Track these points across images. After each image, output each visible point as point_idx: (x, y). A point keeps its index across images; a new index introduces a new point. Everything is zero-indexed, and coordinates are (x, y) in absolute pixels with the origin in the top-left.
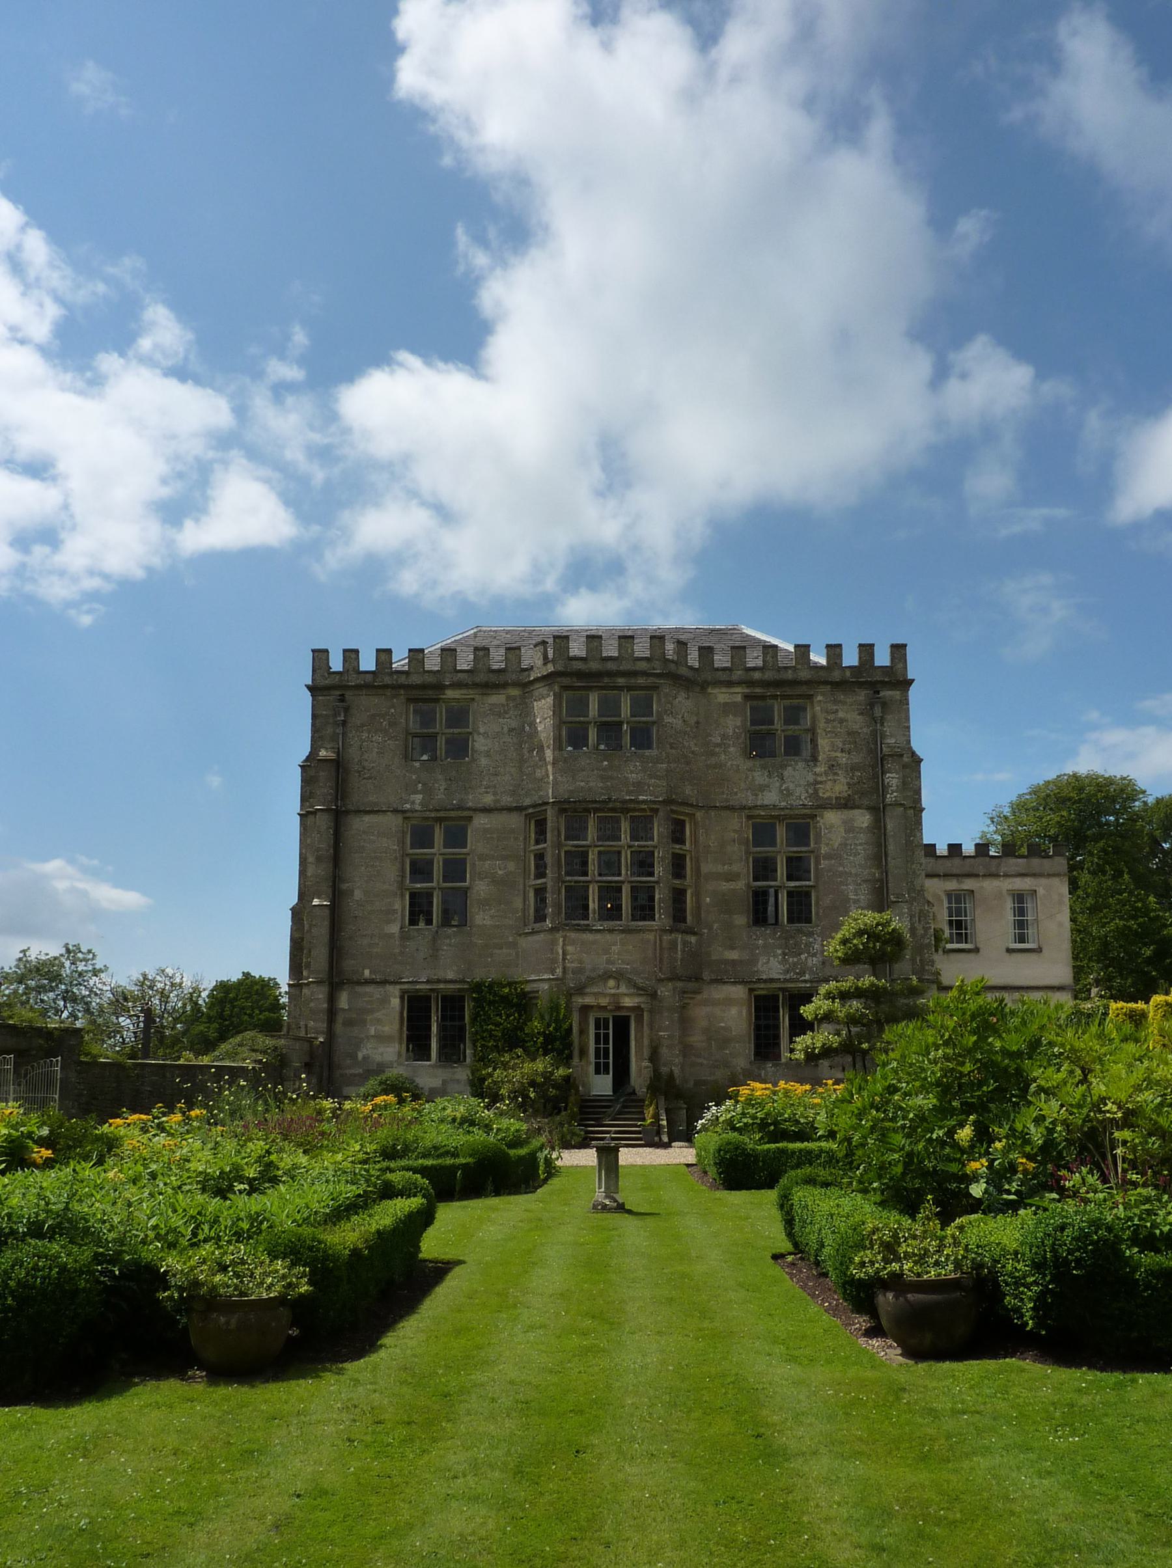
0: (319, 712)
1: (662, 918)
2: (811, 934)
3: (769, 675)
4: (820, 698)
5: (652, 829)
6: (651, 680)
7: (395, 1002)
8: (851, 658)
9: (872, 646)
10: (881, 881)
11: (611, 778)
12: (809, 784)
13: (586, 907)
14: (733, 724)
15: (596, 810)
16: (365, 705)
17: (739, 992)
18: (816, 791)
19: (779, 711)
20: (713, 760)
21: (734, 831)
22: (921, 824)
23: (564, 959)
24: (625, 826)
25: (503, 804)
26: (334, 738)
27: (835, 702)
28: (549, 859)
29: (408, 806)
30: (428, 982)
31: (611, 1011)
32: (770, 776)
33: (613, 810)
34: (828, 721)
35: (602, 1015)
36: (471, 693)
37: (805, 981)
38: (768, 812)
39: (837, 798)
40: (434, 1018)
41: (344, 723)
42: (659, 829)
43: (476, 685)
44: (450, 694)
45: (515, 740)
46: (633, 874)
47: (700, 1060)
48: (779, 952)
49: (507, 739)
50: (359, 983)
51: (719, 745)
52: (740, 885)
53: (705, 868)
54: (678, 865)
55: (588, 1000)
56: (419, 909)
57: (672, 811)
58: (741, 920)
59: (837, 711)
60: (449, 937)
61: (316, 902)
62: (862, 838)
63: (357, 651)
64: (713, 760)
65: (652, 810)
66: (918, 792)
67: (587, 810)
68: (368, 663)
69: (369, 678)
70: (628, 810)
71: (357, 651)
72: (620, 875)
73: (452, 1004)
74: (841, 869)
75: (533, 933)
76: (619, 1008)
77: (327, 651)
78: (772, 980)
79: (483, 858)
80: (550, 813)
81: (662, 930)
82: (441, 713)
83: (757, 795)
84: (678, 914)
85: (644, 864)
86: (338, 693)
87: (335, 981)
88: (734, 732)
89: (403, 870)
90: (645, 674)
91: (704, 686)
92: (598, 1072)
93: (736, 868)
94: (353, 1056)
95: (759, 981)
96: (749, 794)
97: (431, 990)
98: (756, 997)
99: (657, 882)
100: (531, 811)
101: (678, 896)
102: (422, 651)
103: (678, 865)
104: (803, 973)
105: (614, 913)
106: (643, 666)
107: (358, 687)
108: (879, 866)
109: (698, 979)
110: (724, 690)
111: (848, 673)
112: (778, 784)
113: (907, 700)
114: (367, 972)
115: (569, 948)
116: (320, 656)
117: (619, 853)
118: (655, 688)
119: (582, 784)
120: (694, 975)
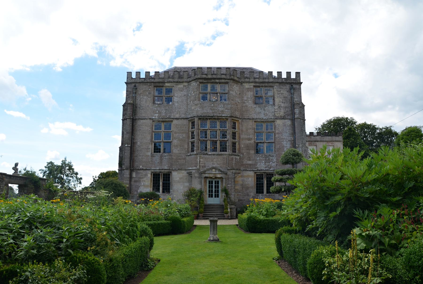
1: (229, 151)
2: (273, 156)
3: (261, 80)
4: (276, 87)
5: (226, 124)
6: (227, 80)
8: (284, 76)
10: (293, 140)
11: (214, 109)
12: (273, 112)
14: (250, 94)
15: (210, 119)
17: (252, 174)
18: (275, 114)
20: (244, 105)
22: (305, 124)
24: (218, 124)
29: (154, 117)
30: (159, 170)
33: (215, 119)
34: (278, 94)
35: (211, 180)
38: (261, 120)
39: (281, 116)
40: (161, 180)
42: (228, 125)
43: (174, 82)
44: (167, 84)
47: (240, 194)
48: (264, 161)
50: (139, 170)
51: (246, 100)
52: (252, 141)
53: (242, 137)
54: (234, 134)
55: (207, 175)
57: (232, 119)
58: (252, 152)
60: (165, 156)
61: (126, 145)
62: (288, 128)
65: (226, 119)
66: (304, 115)
67: (207, 119)
68: (143, 76)
69: (143, 80)
70: (219, 119)
72: (216, 138)
75: (190, 155)
76: (216, 178)
78: (261, 170)
79: (176, 133)
80: (196, 119)
82: (164, 90)
84: (234, 151)
90: (225, 79)
91: (242, 83)
92: (209, 197)
93: (251, 136)
94: (137, 191)
97: (160, 172)
99: (228, 140)
100: (190, 119)
101: (234, 144)
103: (234, 134)
104: (270, 168)
105: (215, 149)
106: (223, 76)
107: (140, 83)
108: (293, 136)
110: (248, 84)
111: (284, 80)
113: (301, 88)
114: (141, 167)
115: (201, 160)
116: (129, 74)
117: (216, 132)
118: (227, 83)
120: (239, 169)
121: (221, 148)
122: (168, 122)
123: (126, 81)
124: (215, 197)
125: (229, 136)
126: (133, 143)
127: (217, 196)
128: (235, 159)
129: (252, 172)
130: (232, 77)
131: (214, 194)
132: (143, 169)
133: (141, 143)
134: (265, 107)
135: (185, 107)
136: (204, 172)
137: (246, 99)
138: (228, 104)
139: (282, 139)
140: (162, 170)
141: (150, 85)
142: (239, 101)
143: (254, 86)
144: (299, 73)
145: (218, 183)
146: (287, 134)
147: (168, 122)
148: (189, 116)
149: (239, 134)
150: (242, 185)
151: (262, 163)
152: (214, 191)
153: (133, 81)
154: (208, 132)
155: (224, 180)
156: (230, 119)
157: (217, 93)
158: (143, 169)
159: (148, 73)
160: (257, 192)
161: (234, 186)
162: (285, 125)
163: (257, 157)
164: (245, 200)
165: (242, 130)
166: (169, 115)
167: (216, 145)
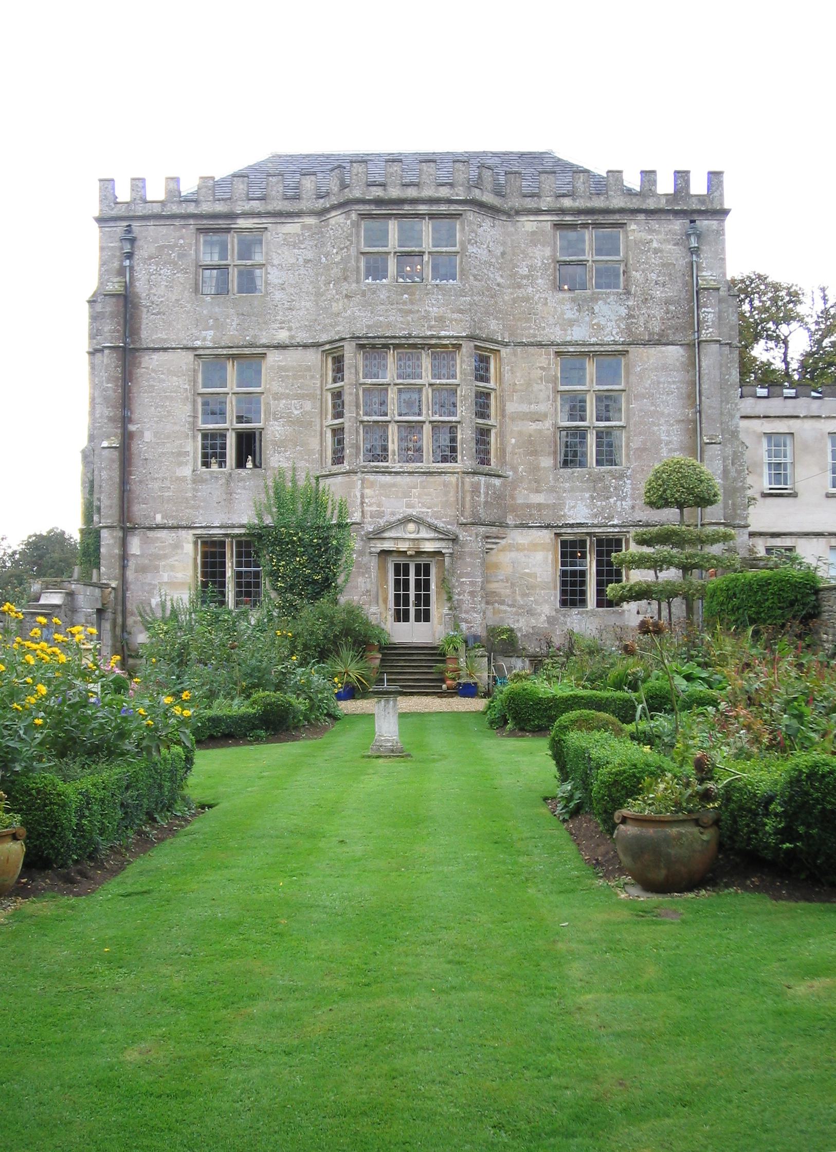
1: (465, 460)
2: (621, 476)
3: (580, 204)
9: (687, 172)
11: (411, 312)
13: (385, 449)
14: (542, 255)
15: (396, 346)
20: (520, 293)
21: (542, 368)
23: (362, 503)
24: (426, 361)
25: (298, 340)
27: (651, 231)
28: (347, 398)
29: (198, 343)
31: (411, 556)
32: (579, 311)
33: (414, 346)
35: (402, 560)
37: (614, 526)
38: (579, 349)
40: (228, 564)
43: (269, 214)
44: (242, 223)
50: (150, 528)
52: (547, 426)
55: (388, 545)
56: (212, 450)
57: (477, 347)
58: (547, 462)
59: (651, 241)
63: (143, 180)
64: (520, 293)
69: (157, 209)
71: (143, 180)
72: (419, 415)
76: (419, 553)
78: (580, 525)
79: (277, 397)
80: (349, 350)
81: (464, 473)
83: (565, 330)
84: (483, 456)
86: (126, 224)
88: (543, 263)
89: (195, 410)
90: (450, 201)
93: (543, 408)
96: (558, 328)
97: (226, 535)
98: (564, 544)
99: (459, 422)
100: (327, 347)
101: (483, 434)
104: (611, 518)
105: (413, 453)
106: (444, 192)
108: (693, 405)
109: (503, 525)
110: (532, 218)
111: (663, 201)
115: (368, 492)
116: (107, 184)
117: (420, 390)
119: (381, 319)
120: (494, 524)
122: (249, 358)
123: (97, 214)
124: (418, 619)
127: (424, 616)
129: (545, 531)
130: (476, 194)
131: (412, 609)
133: (156, 434)
134: (594, 299)
136: (377, 535)
137: (524, 271)
138: (462, 293)
140: (233, 527)
141: (184, 226)
145: (427, 573)
147: (249, 358)
148: (324, 338)
152: (412, 598)
154: (392, 394)
156: (467, 348)
157: (421, 254)
160: (564, 603)
166: (252, 332)
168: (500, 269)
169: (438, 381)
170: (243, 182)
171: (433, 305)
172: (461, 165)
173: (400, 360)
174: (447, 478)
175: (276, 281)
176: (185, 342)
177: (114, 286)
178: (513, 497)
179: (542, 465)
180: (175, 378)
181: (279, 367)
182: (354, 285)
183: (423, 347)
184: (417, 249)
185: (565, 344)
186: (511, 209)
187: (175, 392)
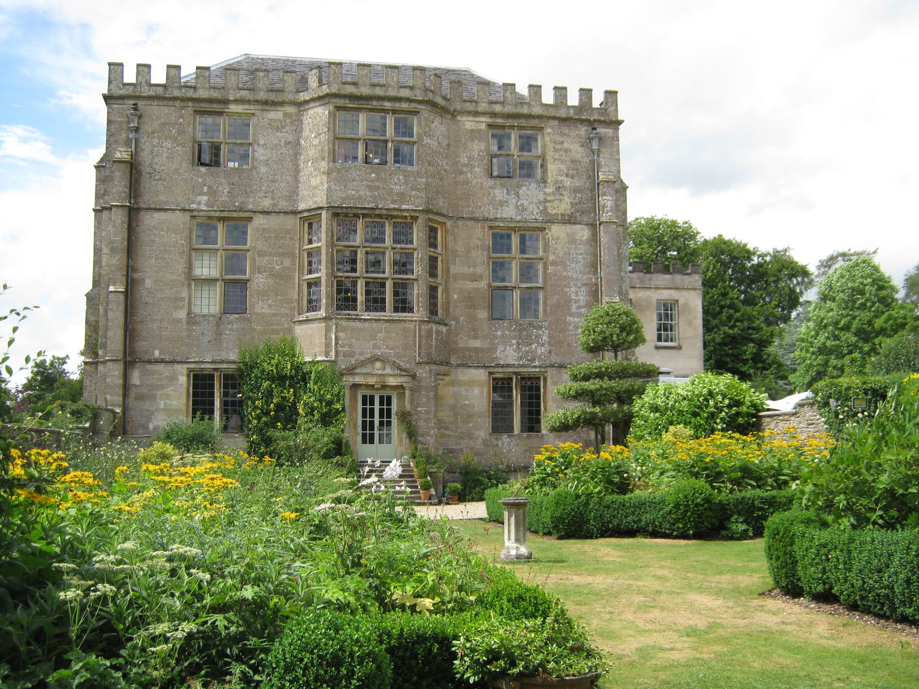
0: (114, 119)
1: (419, 312)
2: (540, 327)
3: (509, 109)
4: (549, 130)
5: (412, 233)
6: (413, 105)
7: (183, 379)
8: (573, 100)
11: (378, 188)
12: (540, 202)
14: (477, 148)
15: (365, 216)
16: (157, 113)
17: (481, 375)
18: (545, 208)
19: (515, 139)
20: (461, 178)
21: (479, 239)
23: (336, 344)
24: (388, 230)
25: (280, 207)
26: (128, 143)
27: (562, 134)
29: (194, 206)
30: (213, 362)
31: (378, 389)
32: (508, 194)
33: (380, 216)
34: (556, 150)
35: (368, 393)
36: (252, 108)
37: (535, 367)
38: (507, 224)
39: (562, 215)
41: (137, 130)
42: (418, 234)
44: (233, 108)
45: (291, 151)
46: (395, 272)
47: (447, 432)
48: (514, 342)
49: (283, 151)
50: (150, 362)
51: (466, 165)
52: (483, 284)
53: (454, 270)
55: (358, 380)
57: (430, 220)
58: (483, 314)
59: (563, 142)
60: (231, 323)
61: (112, 289)
62: (582, 249)
63: (149, 66)
64: (461, 178)
65: (412, 217)
67: (356, 216)
68: (158, 77)
69: (160, 91)
70: (392, 217)
71: (149, 66)
72: (384, 272)
73: (232, 381)
74: (565, 274)
75: (307, 321)
76: (384, 387)
77: (122, 65)
78: (508, 366)
79: (261, 254)
83: (497, 209)
85: (403, 265)
87: (130, 359)
88: (479, 155)
92: (364, 441)
93: (480, 270)
94: (146, 427)
95: (498, 365)
99: (416, 280)
100: (306, 214)
102: (208, 69)
106: (405, 93)
107: (150, 98)
109: (448, 363)
110: (471, 118)
111: (572, 112)
112: (515, 201)
114: (157, 353)
115: (341, 335)
116: (116, 68)
117: (384, 253)
118: (417, 113)
119: (353, 192)
121: (396, 301)
122: (236, 222)
123: (106, 92)
125: (419, 269)
126: (133, 280)
128: (438, 332)
132: (162, 361)
133: (156, 282)
134: (519, 186)
135: (289, 178)
137: (465, 161)
138: (419, 174)
139: (565, 278)
140: (222, 362)
142: (447, 168)
143: (490, 126)
144: (615, 93)
145: (389, 402)
146: (580, 267)
149: (447, 261)
150: (453, 408)
151: (511, 345)
152: (377, 424)
153: (129, 91)
154: (360, 256)
155: (407, 392)
156: (422, 219)
158: (162, 361)
159: (173, 70)
161: (436, 412)
162: (572, 241)
163: (496, 330)
164: (462, 450)
165: (455, 252)
166: (240, 199)
167: (384, 293)
168: (446, 157)
169: (399, 246)
170: (235, 75)
171: (396, 184)
172: (418, 72)
173: (367, 226)
174: (407, 325)
175: (262, 158)
176: (183, 205)
177: (122, 154)
178: (456, 343)
179: (479, 316)
180: (173, 235)
181: (263, 229)
182: (331, 164)
183: (389, 217)
184: (382, 138)
185: (496, 219)
186: (455, 111)
187: (174, 246)
